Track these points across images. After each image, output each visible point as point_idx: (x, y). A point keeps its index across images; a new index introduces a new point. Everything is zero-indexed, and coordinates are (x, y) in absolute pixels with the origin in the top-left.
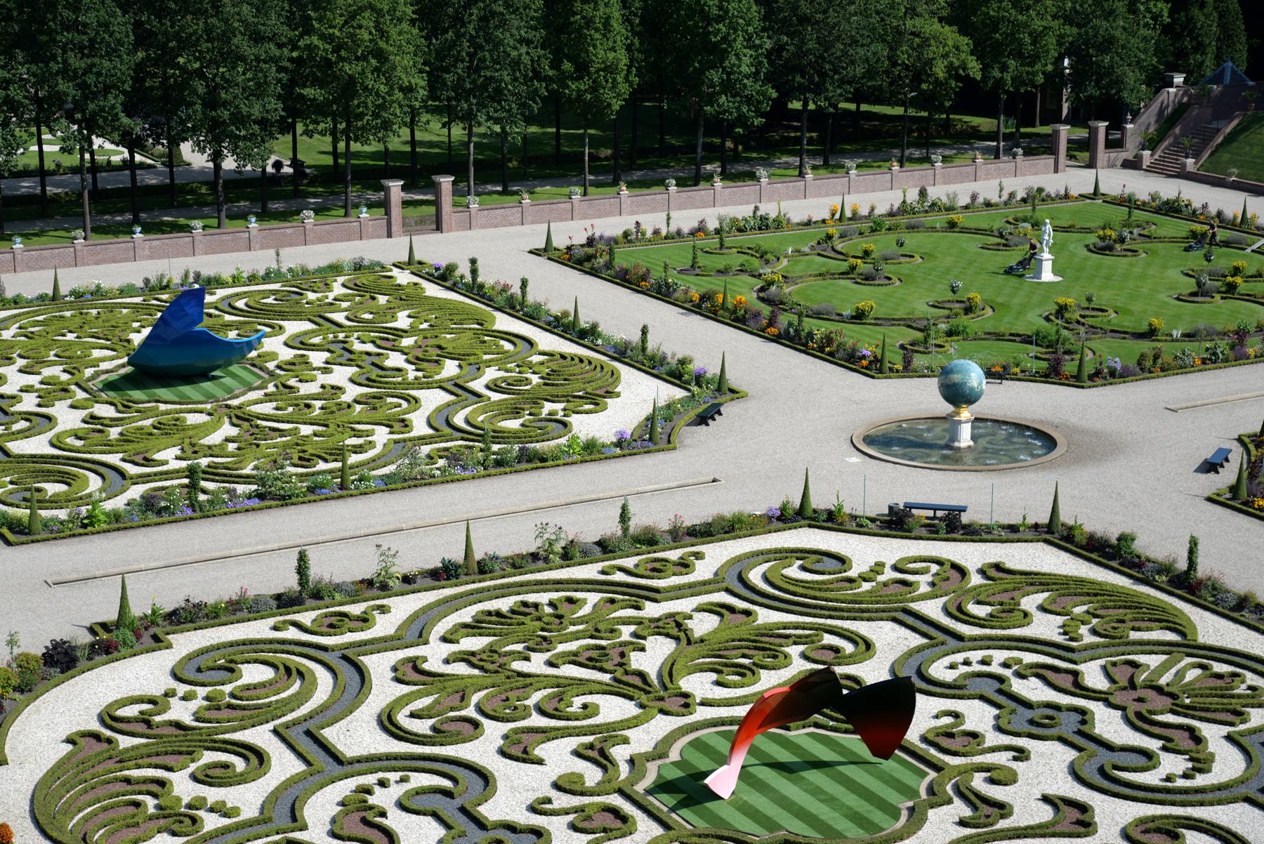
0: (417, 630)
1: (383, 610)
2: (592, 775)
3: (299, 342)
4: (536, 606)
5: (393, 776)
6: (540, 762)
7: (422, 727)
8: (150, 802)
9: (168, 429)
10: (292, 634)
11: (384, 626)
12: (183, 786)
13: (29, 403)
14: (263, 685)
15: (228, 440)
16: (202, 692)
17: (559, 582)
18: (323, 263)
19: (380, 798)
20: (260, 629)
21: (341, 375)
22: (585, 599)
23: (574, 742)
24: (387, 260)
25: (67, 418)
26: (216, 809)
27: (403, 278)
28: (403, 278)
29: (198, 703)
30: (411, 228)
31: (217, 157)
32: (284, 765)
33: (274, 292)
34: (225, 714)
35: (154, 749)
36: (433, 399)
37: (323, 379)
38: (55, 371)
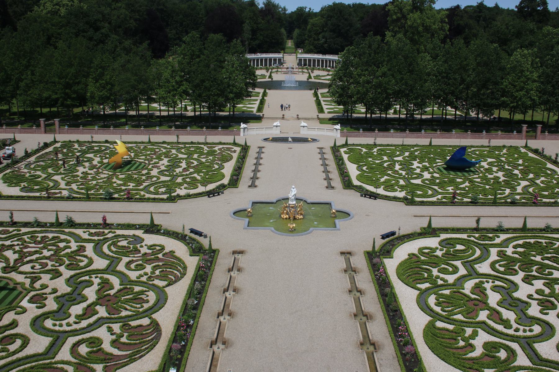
0: (505, 243)
1: (498, 237)
2: (547, 291)
3: (490, 164)
4: (541, 243)
5: (491, 281)
6: (532, 285)
7: (502, 269)
8: (426, 275)
9: (452, 182)
10: (472, 239)
11: (497, 241)
12: (435, 272)
13: (418, 171)
14: (461, 251)
15: (466, 187)
16: (445, 249)
17: (549, 237)
18: (501, 145)
19: (486, 285)
20: (464, 236)
21: (500, 174)
22: (556, 244)
23: (543, 281)
24: (519, 146)
25: (427, 175)
26: (442, 279)
27: (523, 150)
28: (523, 150)
29: (444, 252)
30: (528, 137)
31: (478, 114)
32: (463, 271)
33: (486, 150)
34: (451, 256)
35: (429, 261)
36: (524, 183)
37: (495, 174)
38: (427, 164)
